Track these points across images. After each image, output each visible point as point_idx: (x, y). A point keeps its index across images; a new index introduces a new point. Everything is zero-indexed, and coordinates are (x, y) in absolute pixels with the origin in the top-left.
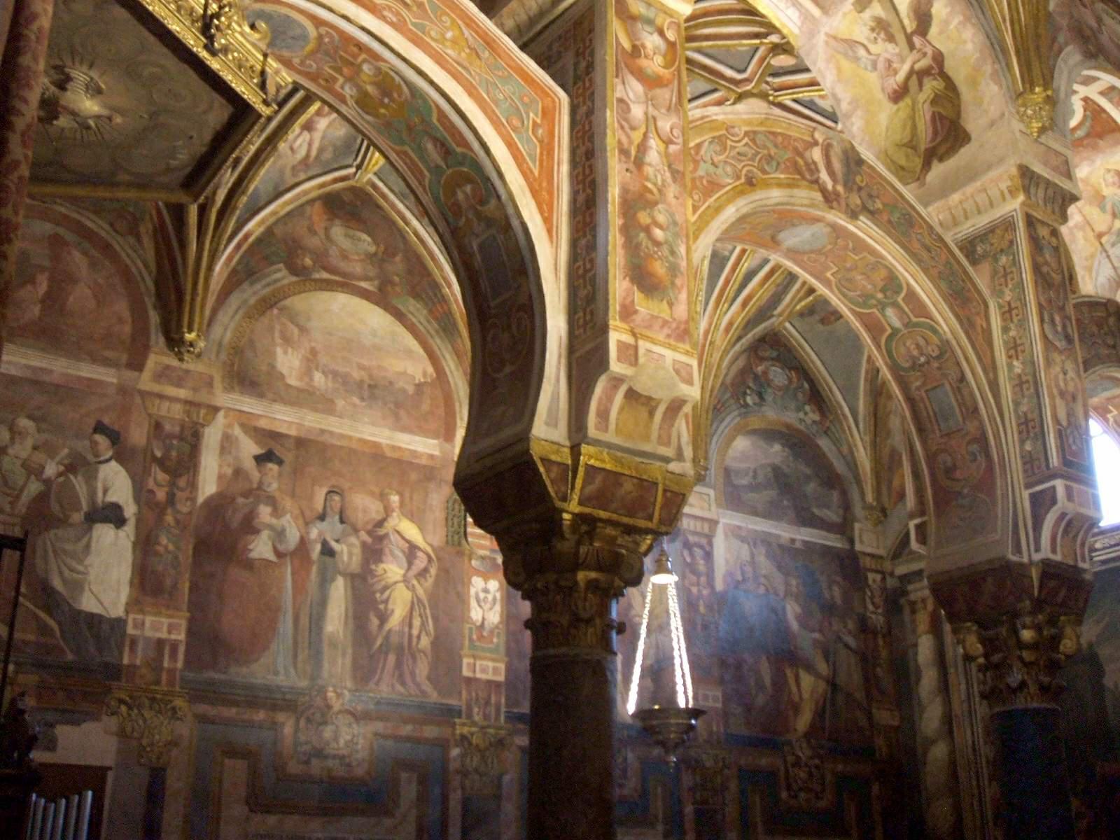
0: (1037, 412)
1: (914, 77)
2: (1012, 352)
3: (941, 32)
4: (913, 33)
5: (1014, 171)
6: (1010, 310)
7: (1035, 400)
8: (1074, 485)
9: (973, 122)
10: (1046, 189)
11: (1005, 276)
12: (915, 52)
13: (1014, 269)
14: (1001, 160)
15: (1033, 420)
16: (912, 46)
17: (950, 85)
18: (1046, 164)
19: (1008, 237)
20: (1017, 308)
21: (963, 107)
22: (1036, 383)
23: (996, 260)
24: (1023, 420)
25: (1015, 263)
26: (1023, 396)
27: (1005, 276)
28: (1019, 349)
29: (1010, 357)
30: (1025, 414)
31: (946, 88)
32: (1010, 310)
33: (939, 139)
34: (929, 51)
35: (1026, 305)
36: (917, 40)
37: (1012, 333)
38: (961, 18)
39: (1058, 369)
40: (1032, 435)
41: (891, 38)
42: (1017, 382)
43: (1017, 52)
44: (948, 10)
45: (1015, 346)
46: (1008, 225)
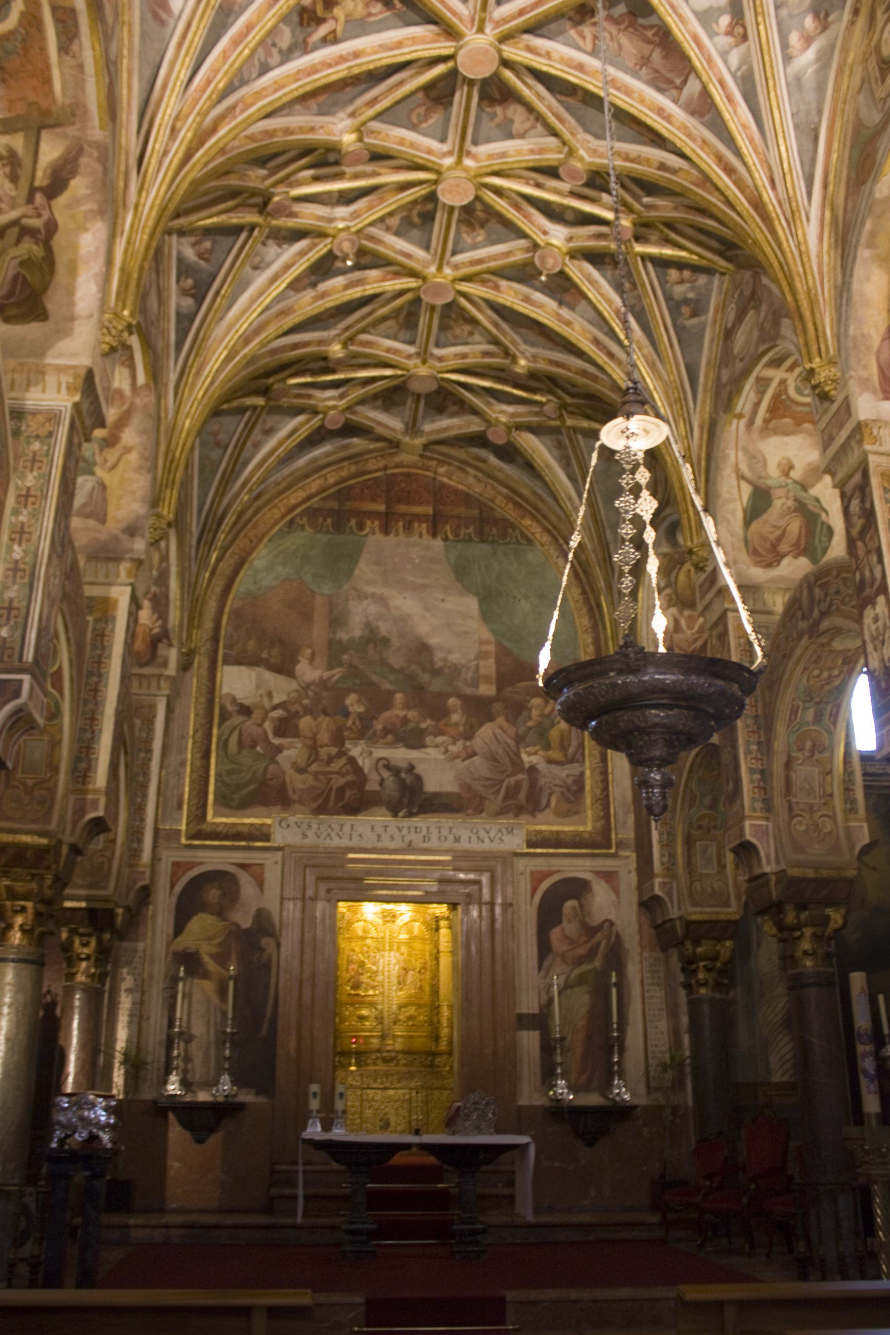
0: (24, 603)
1: (15, 230)
2: (16, 536)
3: (69, 206)
4: (41, 189)
5: (83, 372)
6: (27, 496)
7: (26, 591)
8: (36, 686)
9: (53, 302)
10: (92, 403)
11: (34, 461)
12: (31, 206)
13: (45, 460)
14: (75, 355)
15: (18, 609)
16: (30, 200)
17: (49, 259)
18: (101, 380)
19: (48, 427)
20: (35, 497)
21: (53, 284)
22: (32, 575)
23: (28, 443)
24: (6, 605)
25: (49, 454)
26: (14, 583)
27: (34, 461)
28: (25, 536)
29: (12, 540)
30: (11, 601)
31: (43, 258)
32: (27, 496)
33: (12, 300)
34: (46, 214)
35: (46, 498)
36: (39, 198)
37: (21, 518)
38: (95, 207)
39: (51, 571)
40: (12, 623)
41: (14, 178)
42: (12, 566)
43: (123, 270)
44: (88, 192)
45: (22, 532)
46: (53, 417)
